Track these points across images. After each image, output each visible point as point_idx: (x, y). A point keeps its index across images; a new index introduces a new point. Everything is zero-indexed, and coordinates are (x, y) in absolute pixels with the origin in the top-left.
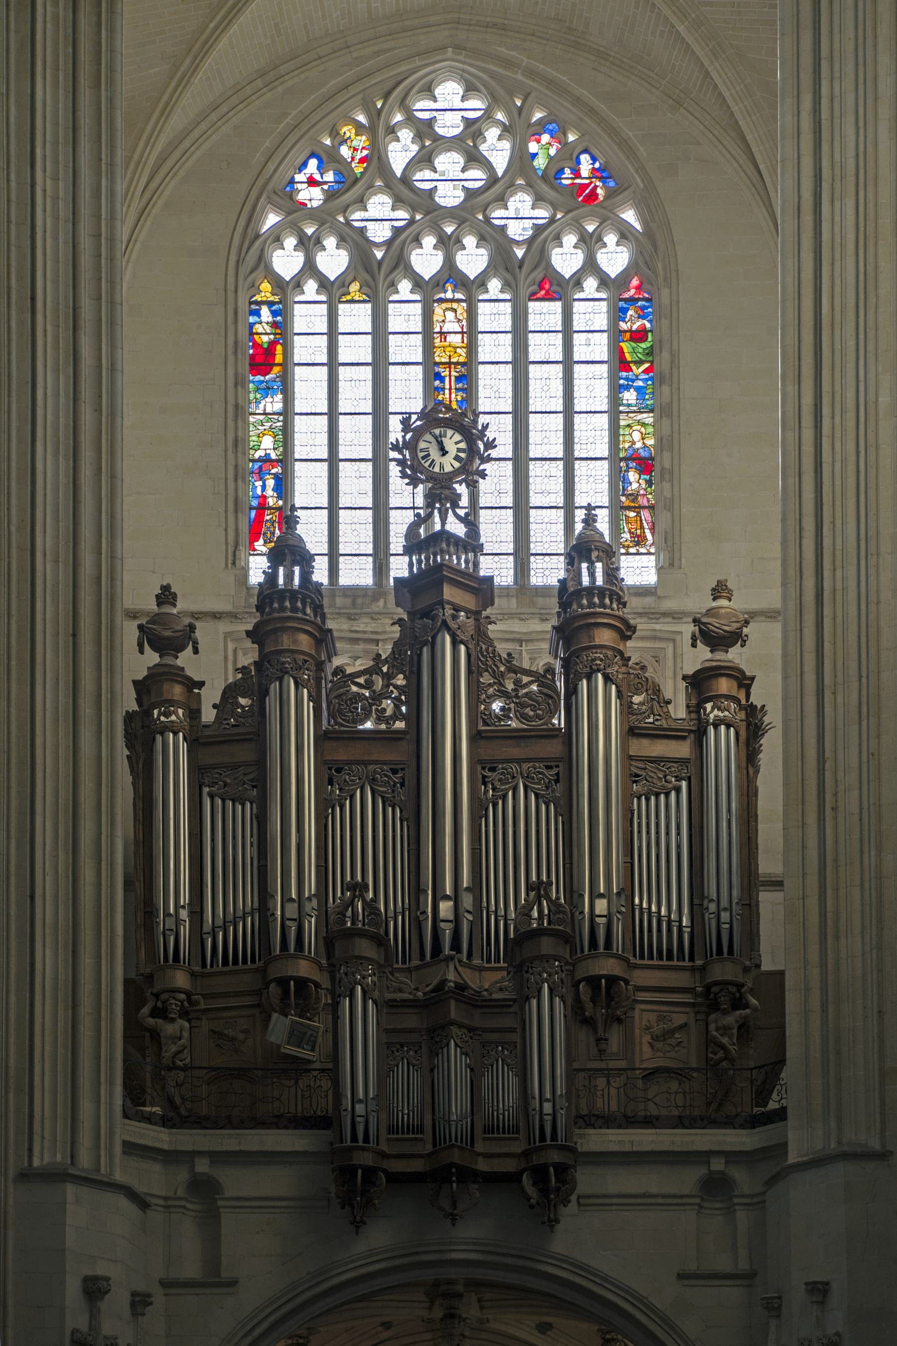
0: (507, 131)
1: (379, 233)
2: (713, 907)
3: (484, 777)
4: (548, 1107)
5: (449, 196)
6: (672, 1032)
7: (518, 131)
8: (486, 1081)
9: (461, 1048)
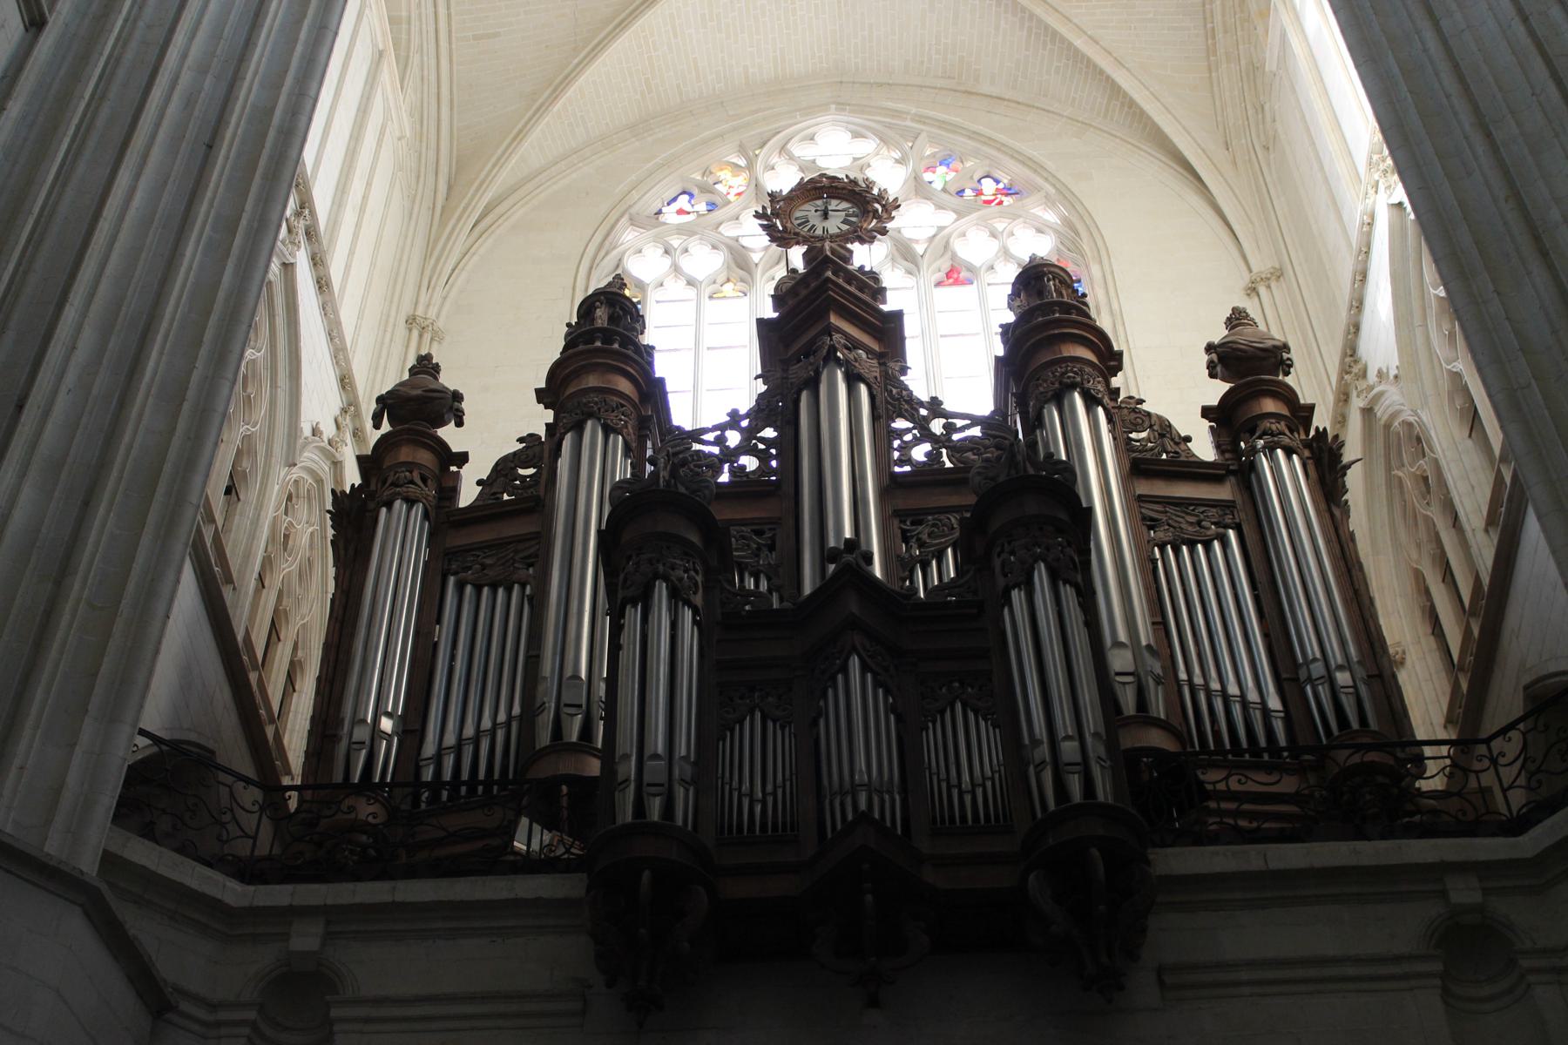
2: (1318, 669)
3: (904, 532)
9: (875, 675)
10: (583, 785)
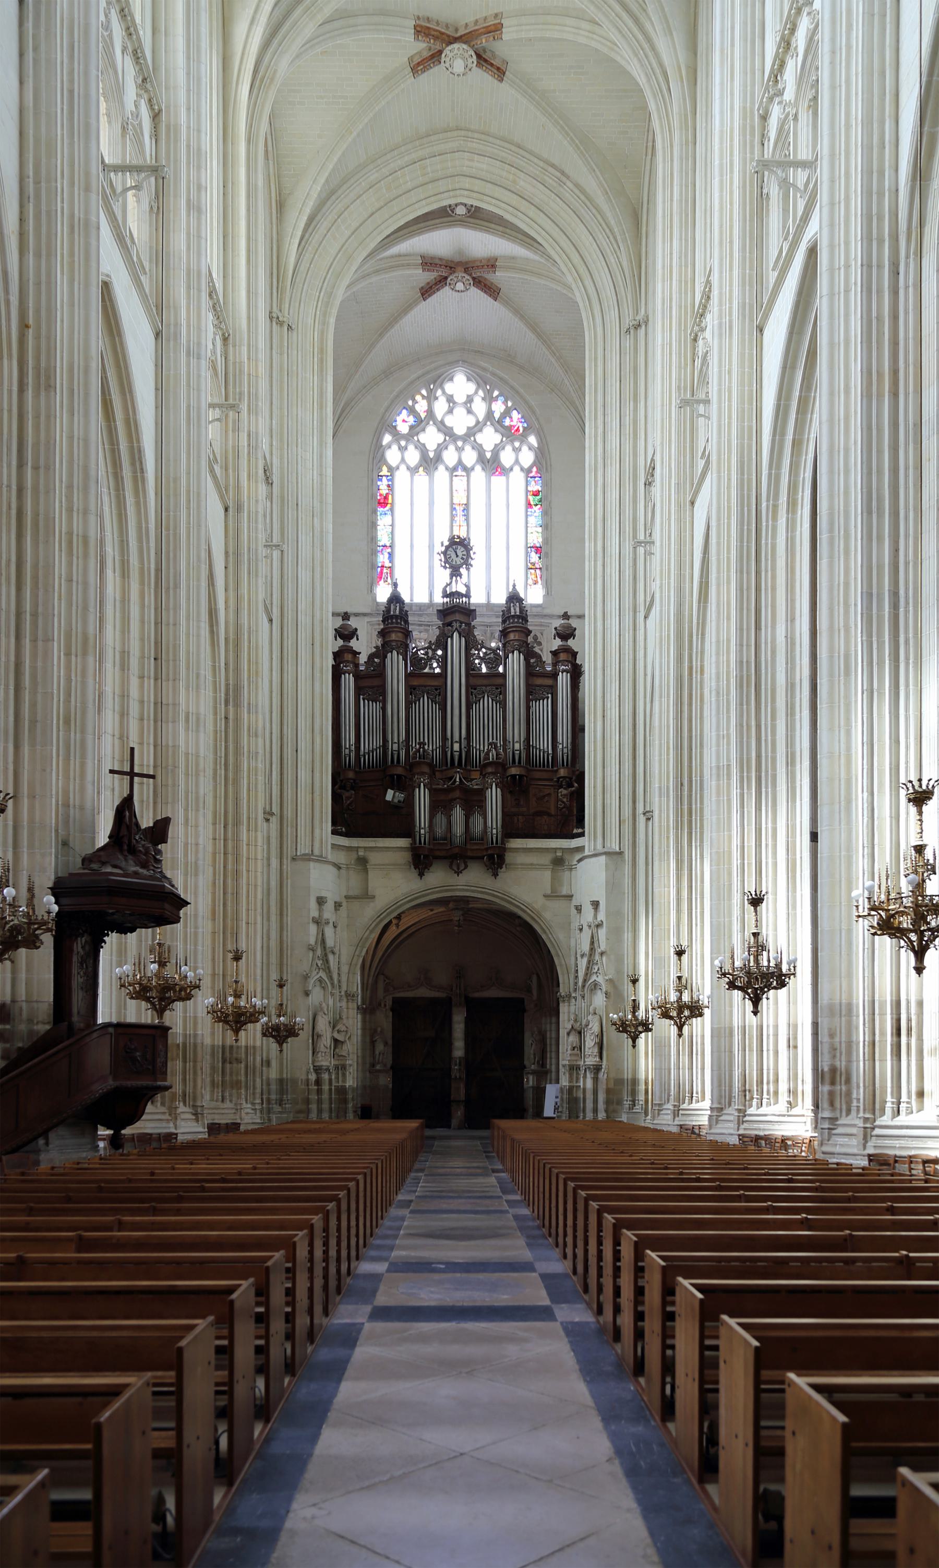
0: (483, 399)
1: (431, 447)
2: (561, 746)
4: (494, 831)
5: (460, 430)
6: (544, 796)
7: (489, 399)
8: (471, 820)
10: (399, 776)
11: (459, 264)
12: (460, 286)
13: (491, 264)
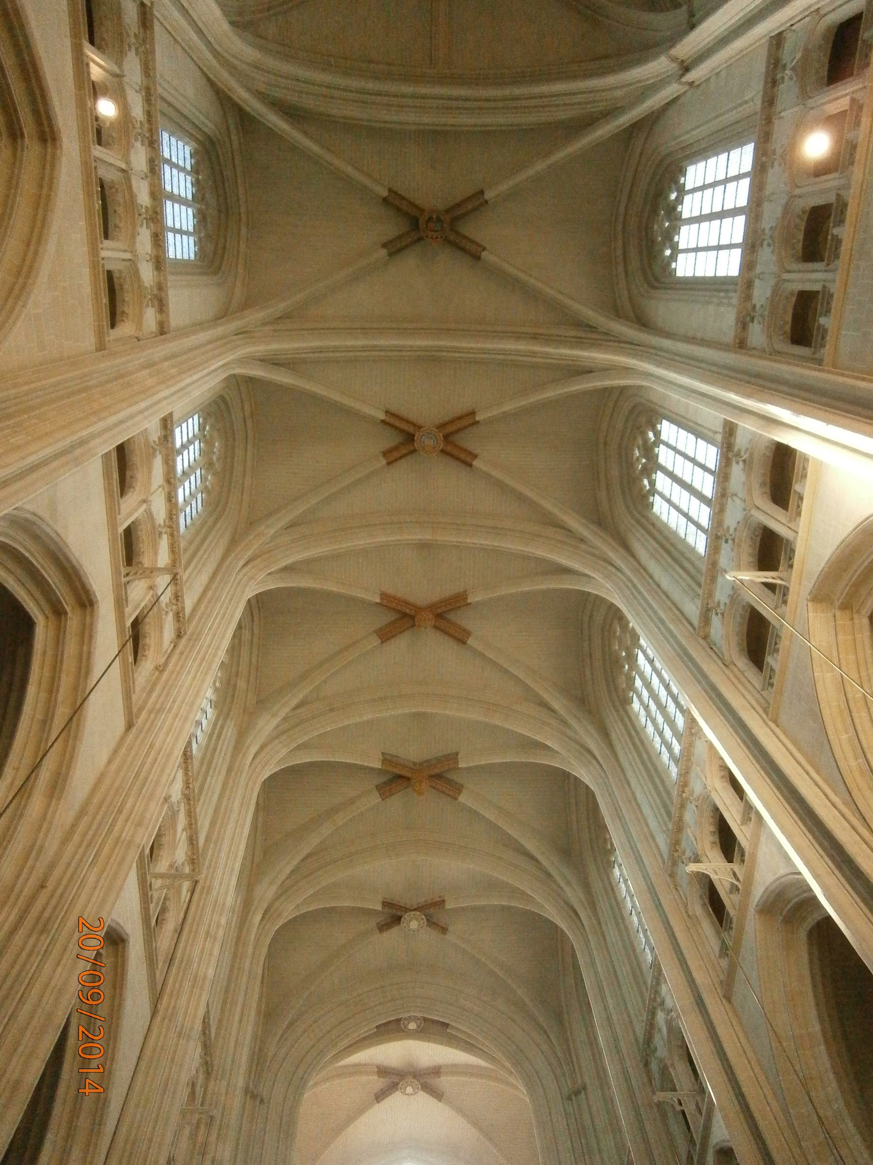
11: (410, 1073)
12: (409, 1090)
13: (436, 1071)
